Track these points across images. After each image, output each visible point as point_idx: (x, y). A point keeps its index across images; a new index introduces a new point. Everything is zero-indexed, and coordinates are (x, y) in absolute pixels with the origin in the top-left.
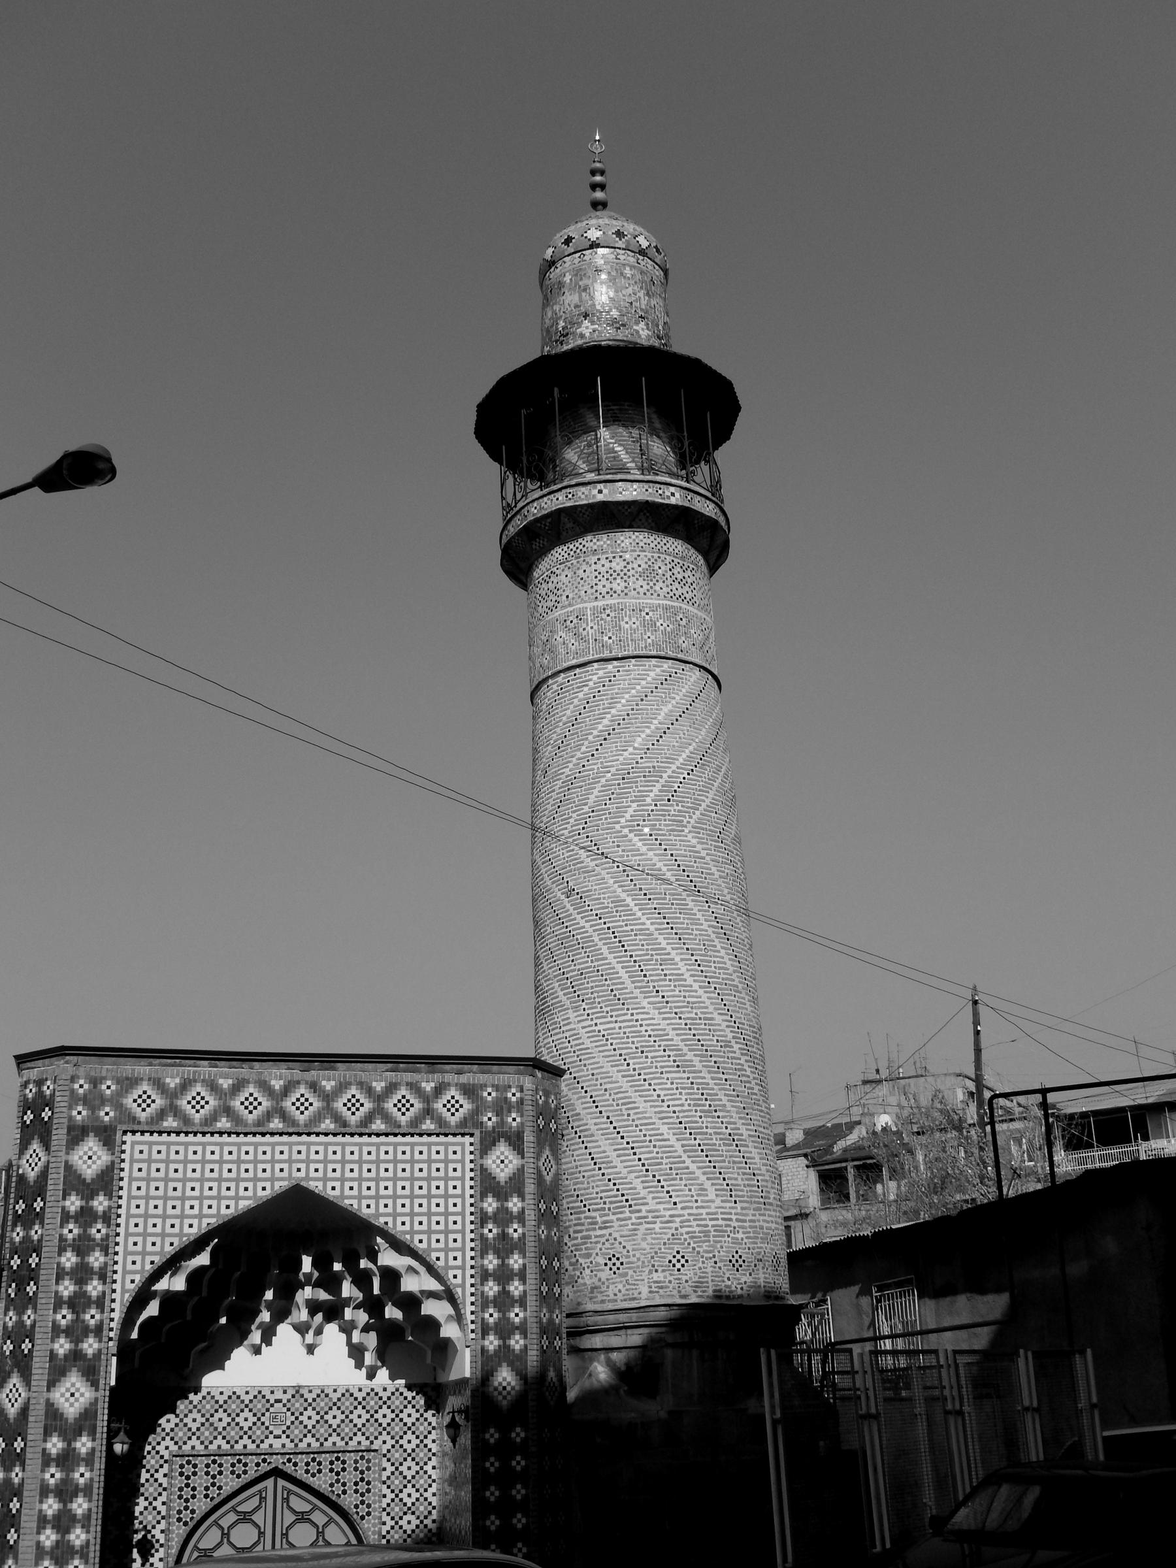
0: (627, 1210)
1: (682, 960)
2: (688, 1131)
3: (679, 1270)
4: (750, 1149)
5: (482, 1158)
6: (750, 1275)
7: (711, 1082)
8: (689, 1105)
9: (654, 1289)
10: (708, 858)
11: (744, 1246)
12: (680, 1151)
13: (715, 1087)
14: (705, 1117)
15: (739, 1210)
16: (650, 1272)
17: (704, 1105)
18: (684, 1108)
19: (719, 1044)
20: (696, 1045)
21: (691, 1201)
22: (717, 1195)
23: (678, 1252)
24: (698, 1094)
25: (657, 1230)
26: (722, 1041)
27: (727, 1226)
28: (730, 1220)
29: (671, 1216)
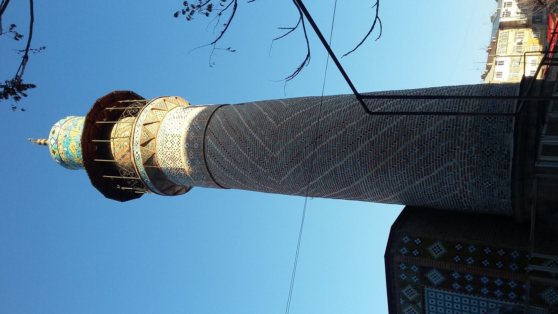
0: (460, 201)
1: (334, 165)
2: (417, 172)
3: (492, 185)
4: (426, 133)
5: (434, 285)
6: (496, 143)
7: (391, 157)
8: (404, 170)
9: (503, 196)
10: (285, 145)
11: (480, 146)
12: (427, 177)
13: (394, 154)
14: (409, 162)
15: (459, 147)
16: (493, 197)
17: (404, 162)
18: (406, 172)
19: (372, 150)
20: (373, 163)
21: (455, 175)
22: (451, 161)
23: (483, 184)
24: (398, 165)
25: (471, 191)
26: (371, 148)
27: (468, 157)
28: (465, 154)
29: (463, 185)
